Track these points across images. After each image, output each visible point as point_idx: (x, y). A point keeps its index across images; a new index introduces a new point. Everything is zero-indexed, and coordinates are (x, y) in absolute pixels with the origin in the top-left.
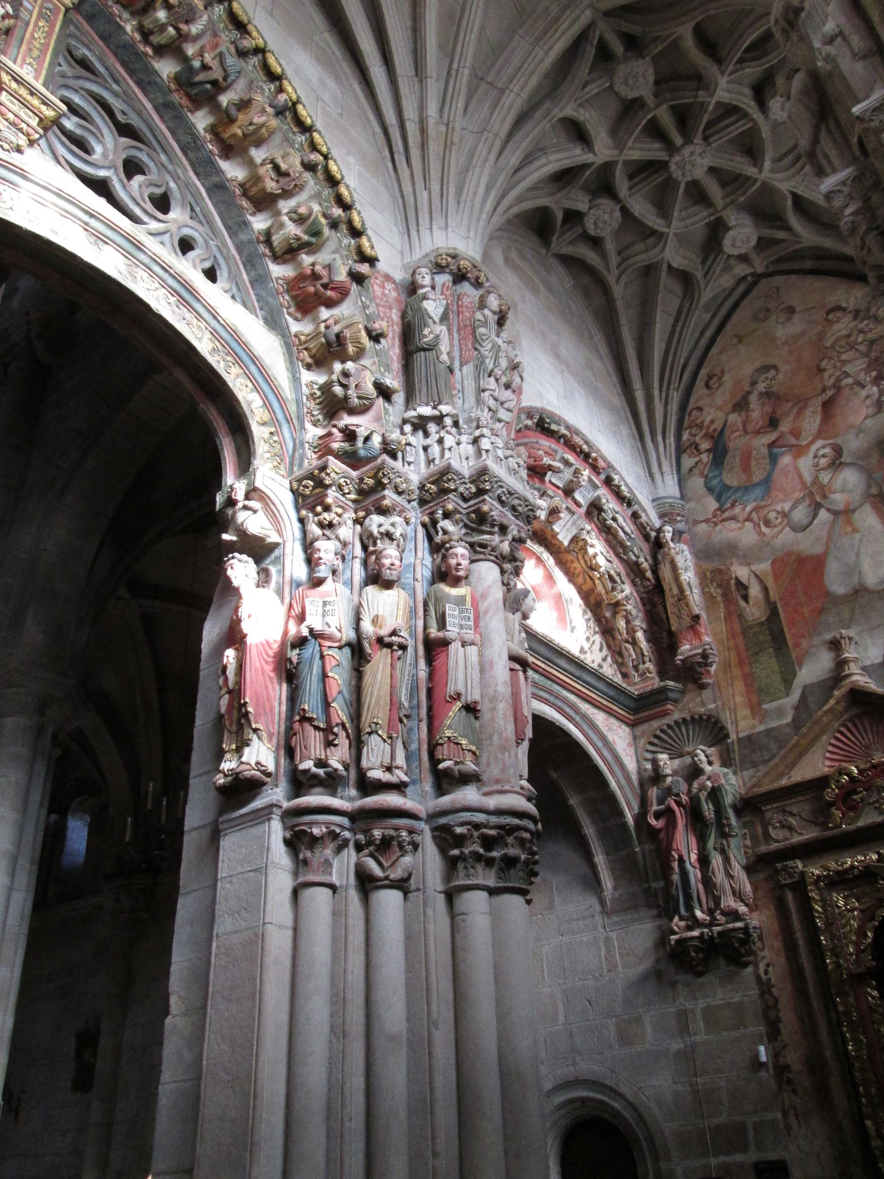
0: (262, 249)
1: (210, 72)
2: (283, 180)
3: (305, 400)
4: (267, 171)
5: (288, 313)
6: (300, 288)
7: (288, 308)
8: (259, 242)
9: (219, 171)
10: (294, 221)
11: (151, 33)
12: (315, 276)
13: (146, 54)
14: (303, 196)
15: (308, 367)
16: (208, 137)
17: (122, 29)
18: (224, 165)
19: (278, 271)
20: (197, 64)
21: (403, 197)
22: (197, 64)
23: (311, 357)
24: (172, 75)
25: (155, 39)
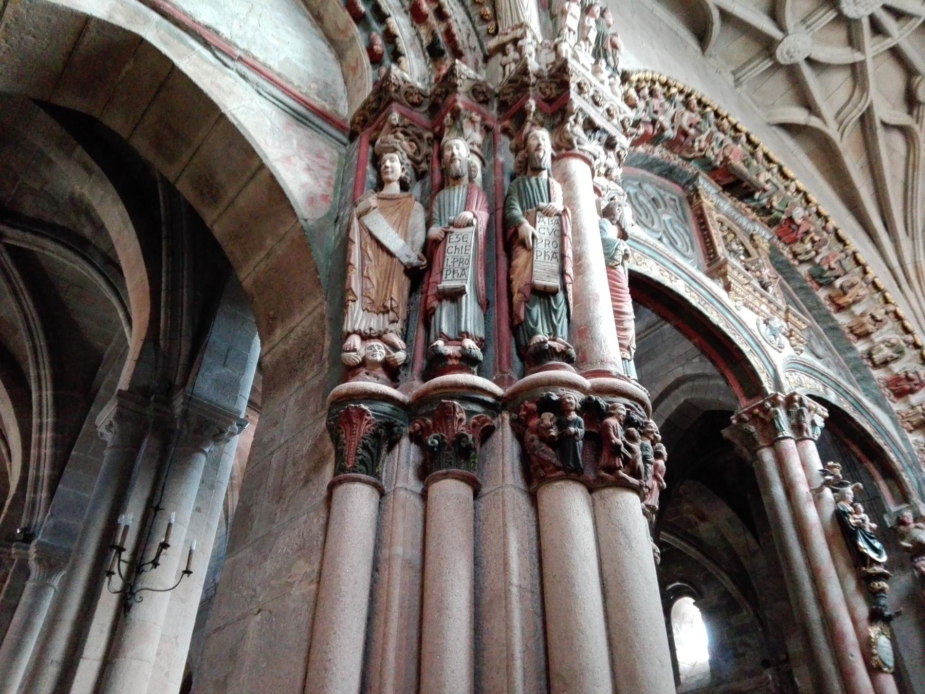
0: (865, 362)
1: (834, 271)
2: (877, 324)
3: (916, 454)
4: (867, 319)
5: (891, 400)
6: (897, 386)
7: (889, 397)
8: (862, 358)
9: (833, 320)
10: (887, 346)
11: (800, 254)
12: (908, 379)
13: (794, 265)
14: (885, 328)
15: (910, 432)
16: (828, 303)
17: (781, 254)
18: (837, 316)
19: (878, 374)
20: (826, 267)
21: (912, 309)
22: (826, 267)
23: (913, 426)
24: (806, 272)
25: (801, 258)
